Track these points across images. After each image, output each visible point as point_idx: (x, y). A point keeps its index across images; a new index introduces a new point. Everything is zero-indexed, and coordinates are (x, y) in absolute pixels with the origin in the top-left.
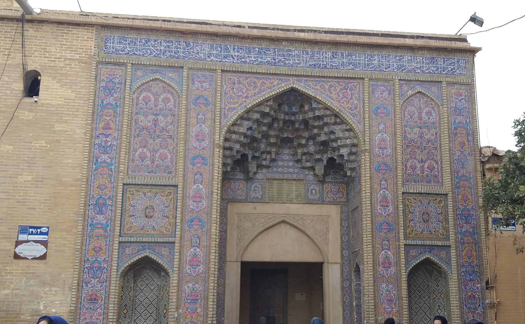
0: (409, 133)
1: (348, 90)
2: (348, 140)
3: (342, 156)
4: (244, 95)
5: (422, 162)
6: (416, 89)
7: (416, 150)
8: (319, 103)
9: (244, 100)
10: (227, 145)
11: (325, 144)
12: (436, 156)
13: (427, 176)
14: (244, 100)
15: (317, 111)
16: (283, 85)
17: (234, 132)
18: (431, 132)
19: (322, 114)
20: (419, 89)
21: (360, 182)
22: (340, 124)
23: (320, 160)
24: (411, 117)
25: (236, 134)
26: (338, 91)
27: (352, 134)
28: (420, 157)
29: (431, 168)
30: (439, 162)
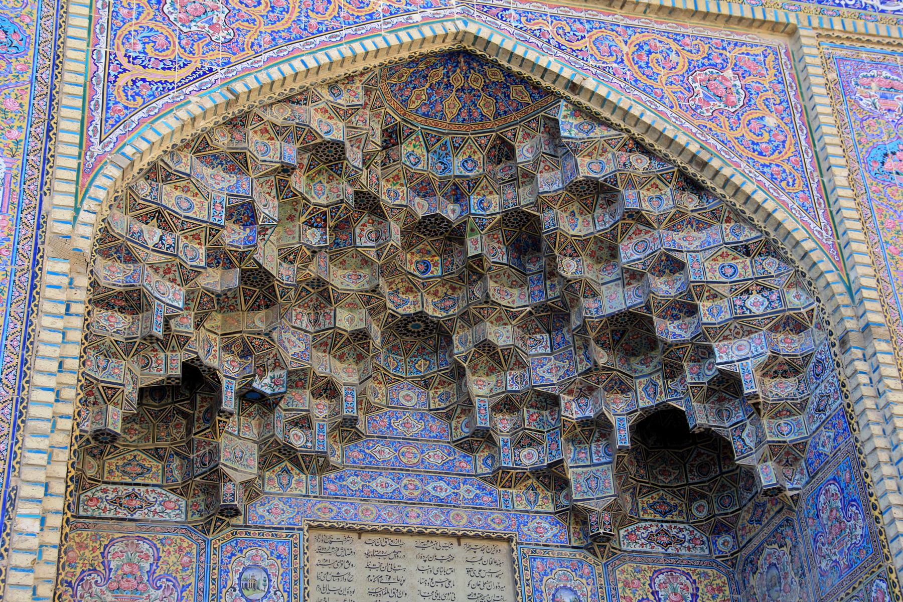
1: (729, 73)
2: (755, 297)
3: (727, 386)
4: (221, 36)
8: (595, 119)
9: (220, 55)
10: (115, 275)
11: (630, 332)
14: (220, 55)
15: (583, 162)
16: (417, 17)
17: (159, 216)
19: (610, 168)
21: (859, 497)
22: (700, 226)
23: (597, 428)
25: (165, 226)
26: (681, 69)
27: (771, 265)
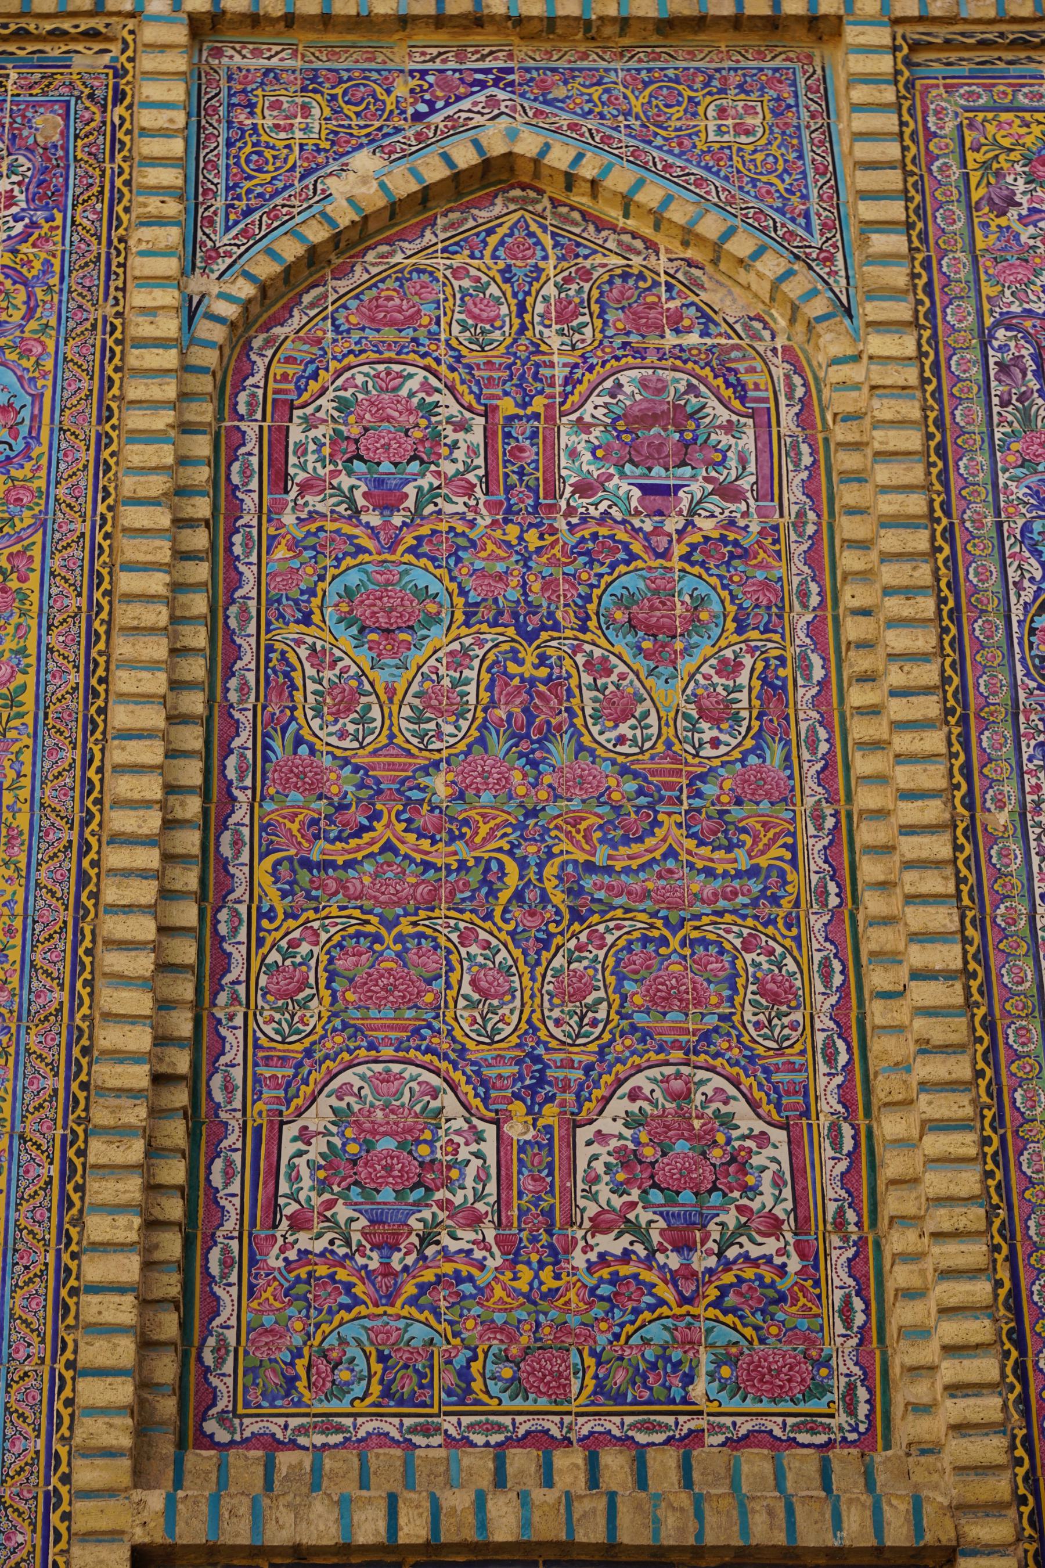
0: (345, 701)
5: (535, 1090)
6: (455, 127)
7: (446, 925)
12: (777, 995)
13: (618, 1291)
18: (699, 659)
20: (505, 131)
24: (386, 497)
28: (509, 1018)
29: (685, 1173)
30: (826, 1090)
